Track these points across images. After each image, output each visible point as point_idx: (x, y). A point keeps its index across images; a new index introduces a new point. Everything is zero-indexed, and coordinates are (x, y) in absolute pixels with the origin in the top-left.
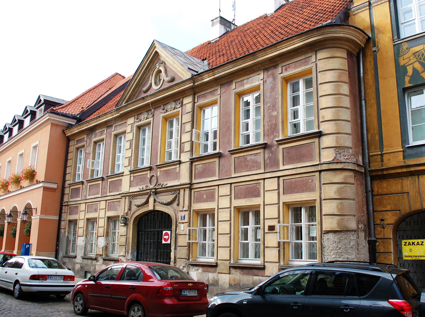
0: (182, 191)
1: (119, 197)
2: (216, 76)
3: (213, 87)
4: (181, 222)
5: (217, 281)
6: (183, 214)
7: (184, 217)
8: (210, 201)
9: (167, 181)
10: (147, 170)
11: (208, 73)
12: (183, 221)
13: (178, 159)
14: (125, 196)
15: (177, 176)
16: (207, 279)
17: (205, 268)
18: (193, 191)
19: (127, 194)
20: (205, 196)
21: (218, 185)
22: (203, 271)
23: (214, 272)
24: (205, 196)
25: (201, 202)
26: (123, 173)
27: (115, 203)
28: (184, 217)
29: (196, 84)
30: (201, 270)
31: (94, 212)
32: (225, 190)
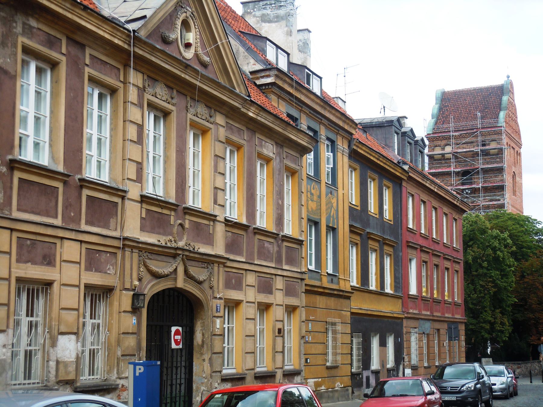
1: (116, 243)
2: (259, 118)
3: (239, 123)
9: (198, 242)
10: (171, 209)
11: (256, 108)
12: (217, 315)
14: (132, 247)
20: (233, 281)
24: (233, 281)
27: (104, 256)
29: (242, 110)
31: (42, 264)
32: (251, 279)
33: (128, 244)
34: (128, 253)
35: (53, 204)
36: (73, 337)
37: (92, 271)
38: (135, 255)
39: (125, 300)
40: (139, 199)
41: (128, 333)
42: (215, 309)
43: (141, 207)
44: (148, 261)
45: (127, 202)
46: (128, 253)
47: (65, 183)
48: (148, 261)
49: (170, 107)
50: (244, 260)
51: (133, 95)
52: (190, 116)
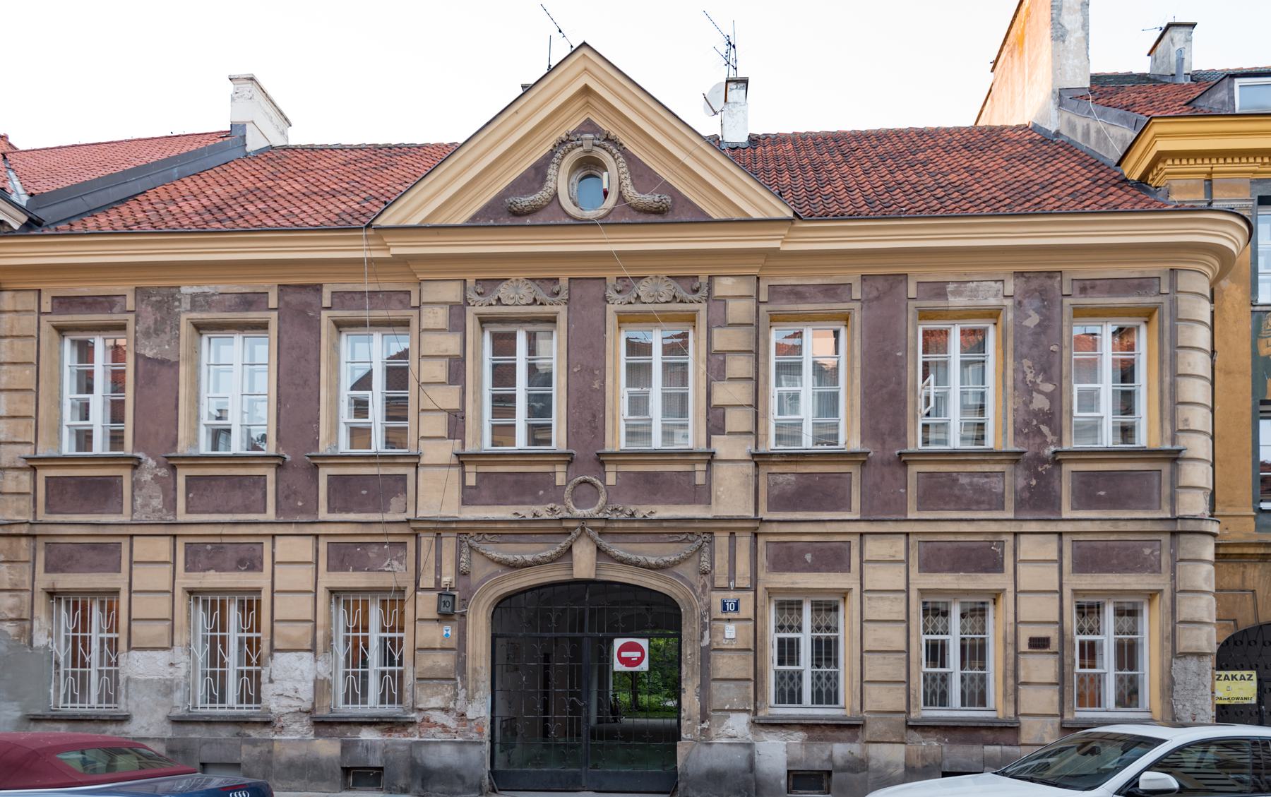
0: (722, 540)
4: (724, 616)
5: (862, 760)
6: (731, 596)
7: (736, 604)
8: (829, 571)
13: (703, 448)
15: (703, 495)
16: (825, 756)
17: (817, 732)
18: (761, 540)
19: (454, 526)
21: (862, 534)
22: (810, 739)
23: (852, 740)
24: (808, 557)
25: (796, 571)
26: (418, 456)
28: (736, 604)
30: (798, 736)
33: (440, 528)
34: (427, 541)
35: (259, 494)
36: (309, 655)
37: (347, 570)
38: (449, 544)
39: (427, 604)
40: (455, 461)
41: (434, 649)
42: (719, 607)
43: (463, 474)
44: (483, 547)
45: (421, 470)
46: (427, 541)
47: (278, 466)
48: (483, 547)
49: (547, 309)
50: (858, 517)
51: (436, 317)
52: (611, 309)
